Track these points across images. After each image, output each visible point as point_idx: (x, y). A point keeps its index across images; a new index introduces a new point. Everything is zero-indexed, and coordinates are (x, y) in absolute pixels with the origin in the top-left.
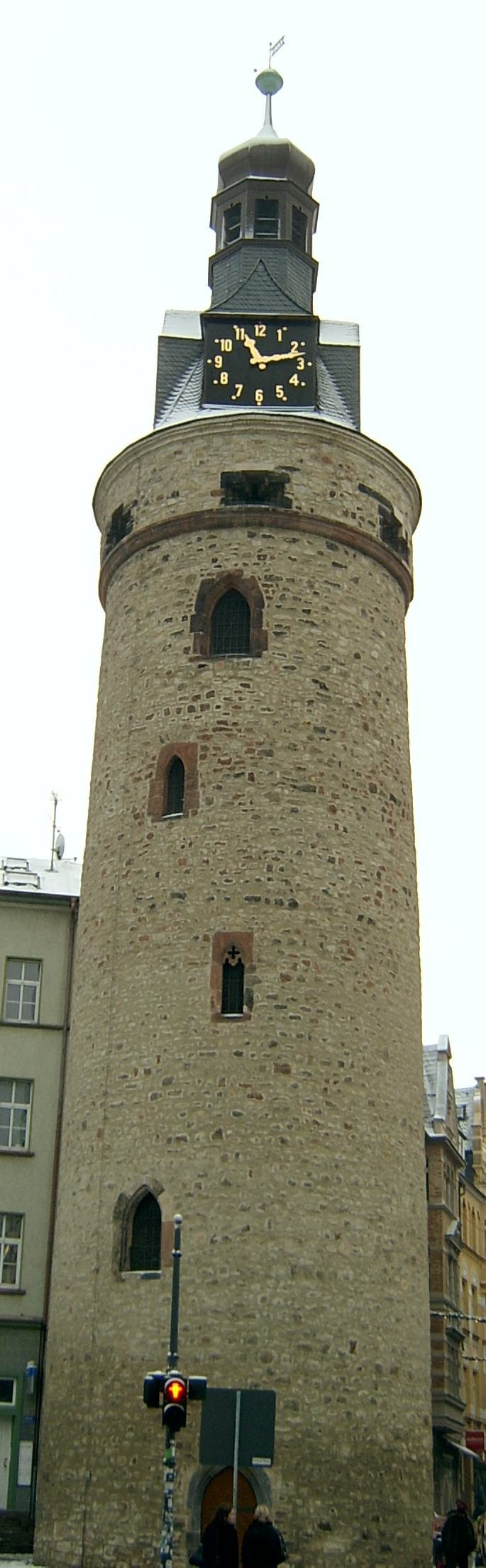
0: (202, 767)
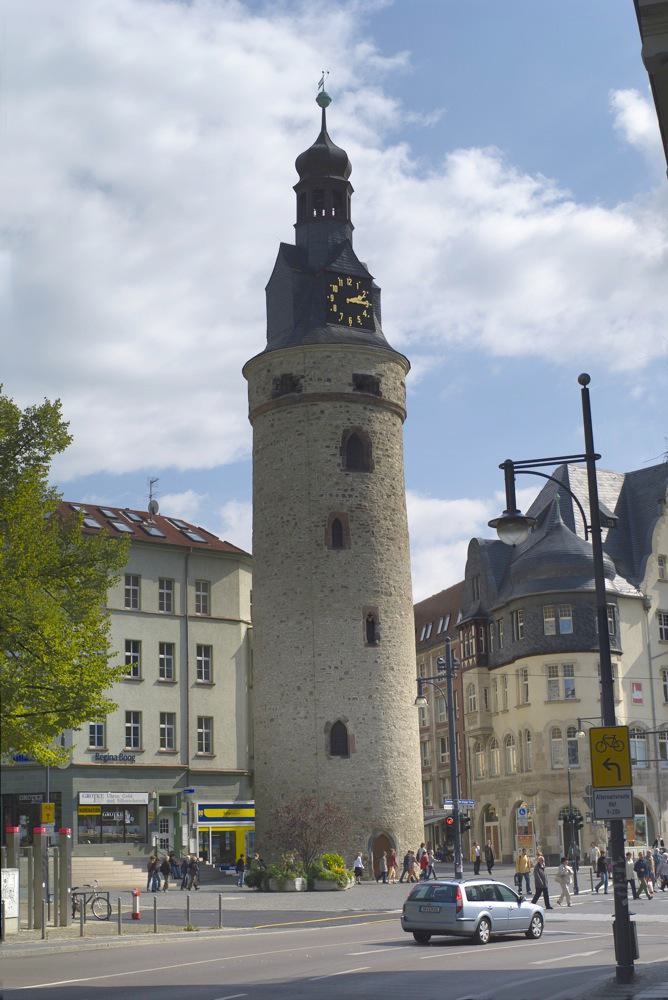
0: (352, 526)
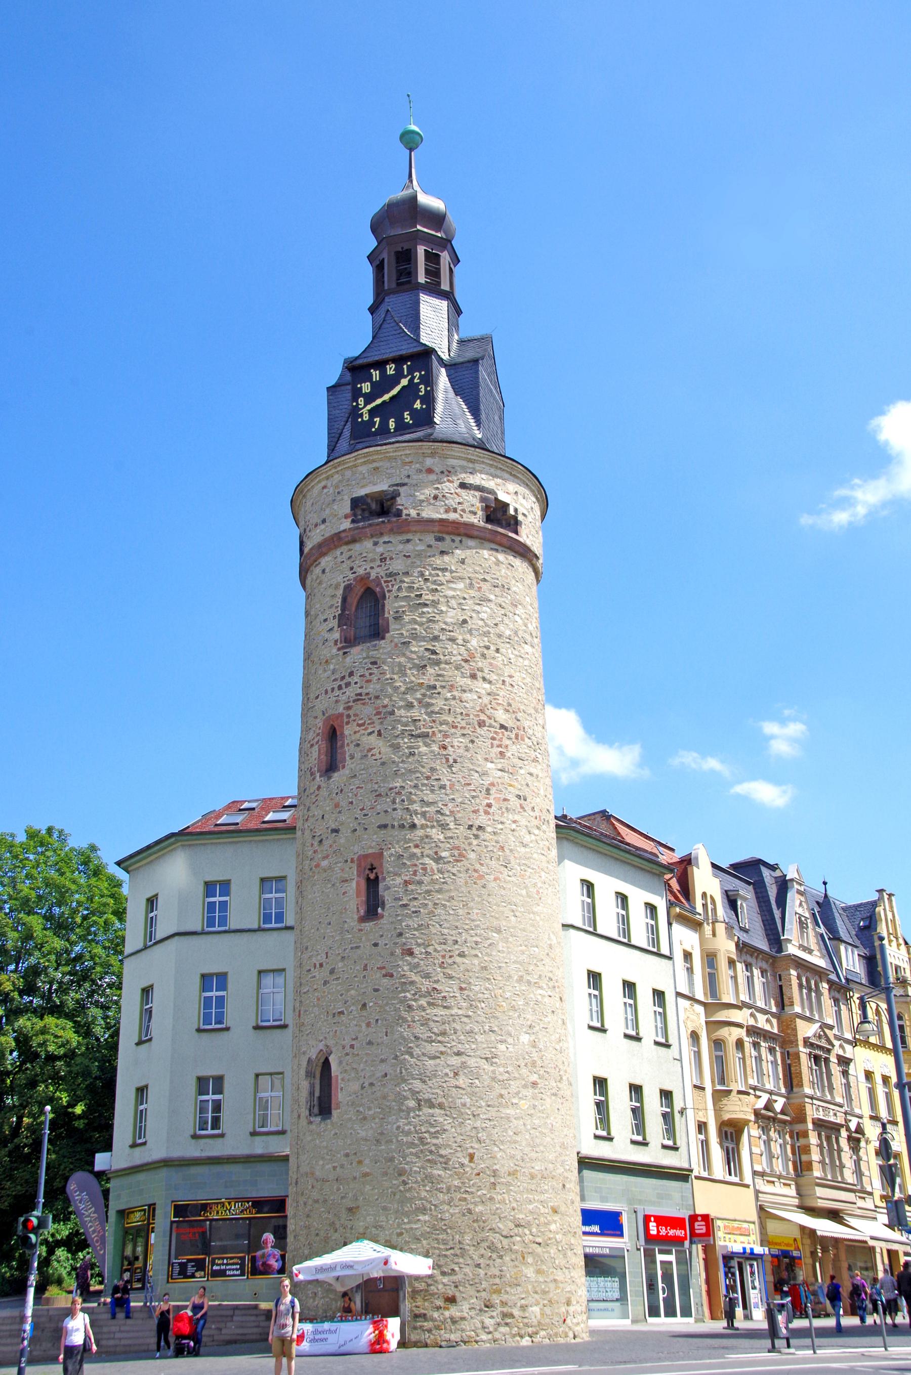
0: (347, 731)
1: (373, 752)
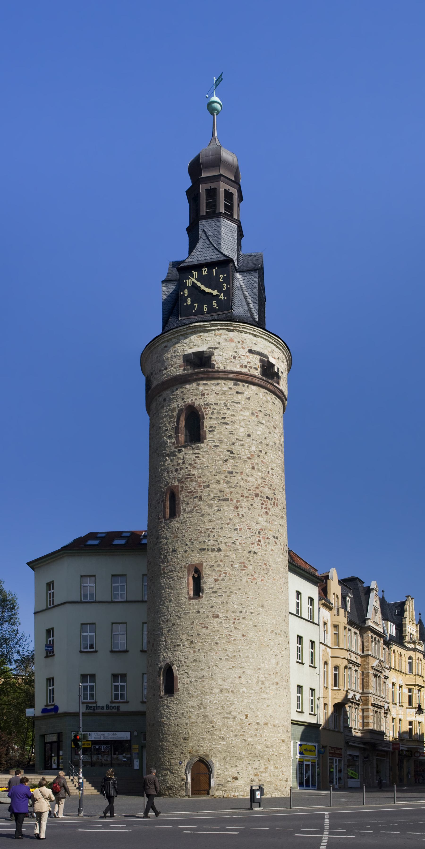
1: (197, 508)
